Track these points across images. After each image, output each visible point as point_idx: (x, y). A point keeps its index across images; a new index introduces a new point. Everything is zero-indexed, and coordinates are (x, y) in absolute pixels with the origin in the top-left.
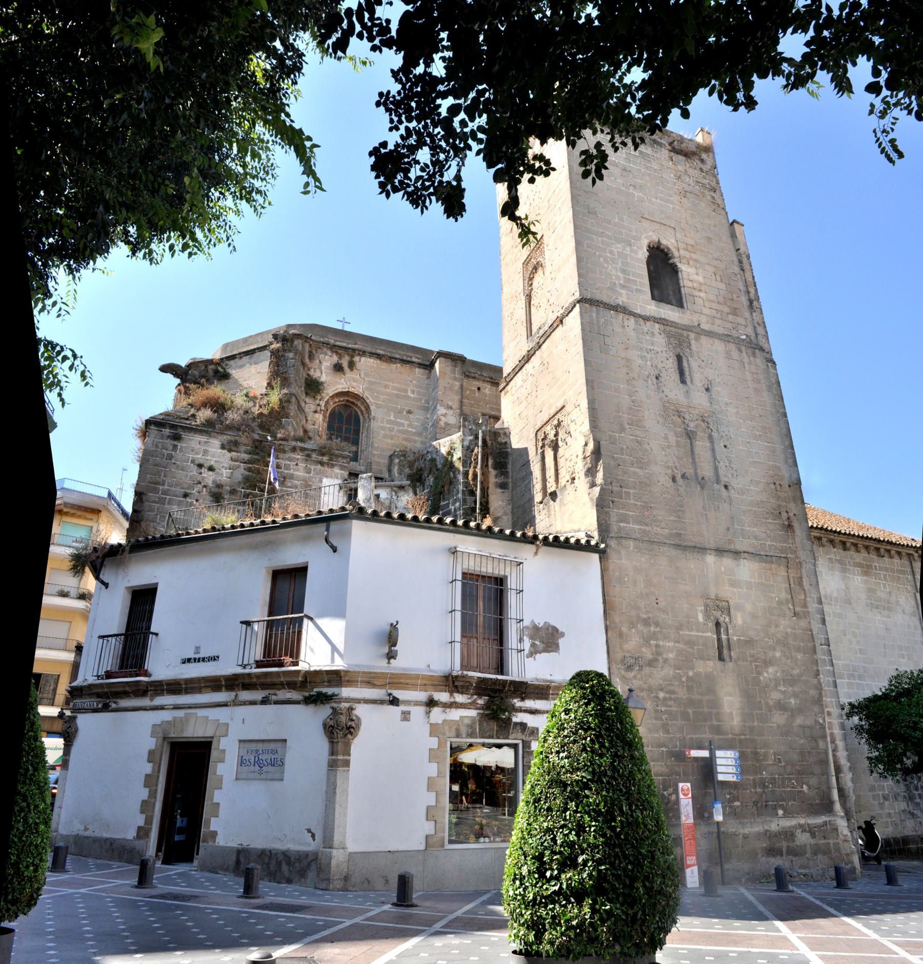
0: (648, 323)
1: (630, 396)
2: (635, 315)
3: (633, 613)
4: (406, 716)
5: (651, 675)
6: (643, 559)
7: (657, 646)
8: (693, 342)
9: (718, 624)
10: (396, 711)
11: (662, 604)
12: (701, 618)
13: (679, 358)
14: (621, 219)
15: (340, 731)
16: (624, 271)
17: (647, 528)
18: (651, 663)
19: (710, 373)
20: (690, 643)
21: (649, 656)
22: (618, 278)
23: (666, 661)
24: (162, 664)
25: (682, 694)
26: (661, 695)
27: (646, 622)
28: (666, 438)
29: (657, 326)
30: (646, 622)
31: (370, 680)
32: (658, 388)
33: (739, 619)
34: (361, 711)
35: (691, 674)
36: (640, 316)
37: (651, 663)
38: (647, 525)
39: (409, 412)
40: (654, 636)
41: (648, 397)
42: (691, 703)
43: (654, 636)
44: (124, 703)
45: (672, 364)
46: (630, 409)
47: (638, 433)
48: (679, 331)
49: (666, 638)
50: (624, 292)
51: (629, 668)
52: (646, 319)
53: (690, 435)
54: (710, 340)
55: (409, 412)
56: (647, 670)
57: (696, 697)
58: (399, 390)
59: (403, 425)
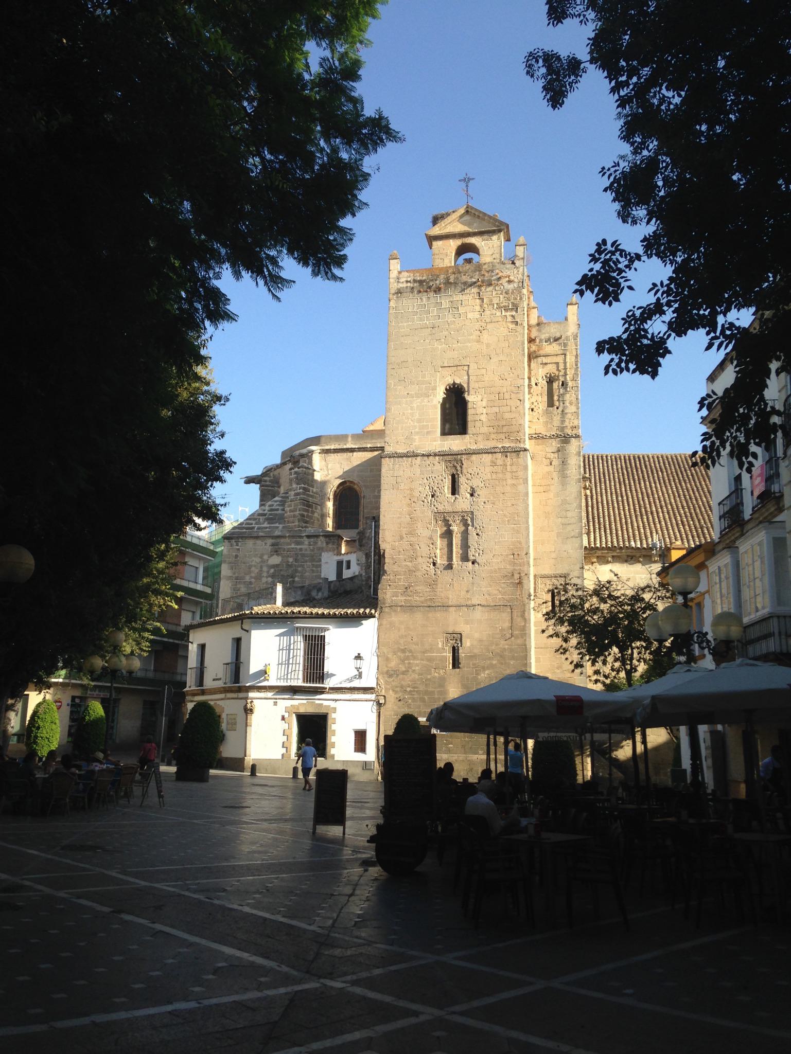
3: (396, 646)
4: (275, 704)
5: (403, 679)
7: (409, 663)
11: (415, 640)
12: (440, 646)
13: (453, 476)
19: (475, 483)
20: (430, 660)
21: (404, 669)
23: (414, 671)
25: (422, 688)
26: (408, 689)
27: (403, 651)
29: (437, 458)
30: (403, 651)
33: (467, 643)
35: (429, 677)
36: (423, 455)
37: (404, 673)
40: (407, 658)
42: (426, 693)
43: (407, 658)
47: (412, 539)
49: (415, 658)
50: (417, 437)
57: (430, 689)
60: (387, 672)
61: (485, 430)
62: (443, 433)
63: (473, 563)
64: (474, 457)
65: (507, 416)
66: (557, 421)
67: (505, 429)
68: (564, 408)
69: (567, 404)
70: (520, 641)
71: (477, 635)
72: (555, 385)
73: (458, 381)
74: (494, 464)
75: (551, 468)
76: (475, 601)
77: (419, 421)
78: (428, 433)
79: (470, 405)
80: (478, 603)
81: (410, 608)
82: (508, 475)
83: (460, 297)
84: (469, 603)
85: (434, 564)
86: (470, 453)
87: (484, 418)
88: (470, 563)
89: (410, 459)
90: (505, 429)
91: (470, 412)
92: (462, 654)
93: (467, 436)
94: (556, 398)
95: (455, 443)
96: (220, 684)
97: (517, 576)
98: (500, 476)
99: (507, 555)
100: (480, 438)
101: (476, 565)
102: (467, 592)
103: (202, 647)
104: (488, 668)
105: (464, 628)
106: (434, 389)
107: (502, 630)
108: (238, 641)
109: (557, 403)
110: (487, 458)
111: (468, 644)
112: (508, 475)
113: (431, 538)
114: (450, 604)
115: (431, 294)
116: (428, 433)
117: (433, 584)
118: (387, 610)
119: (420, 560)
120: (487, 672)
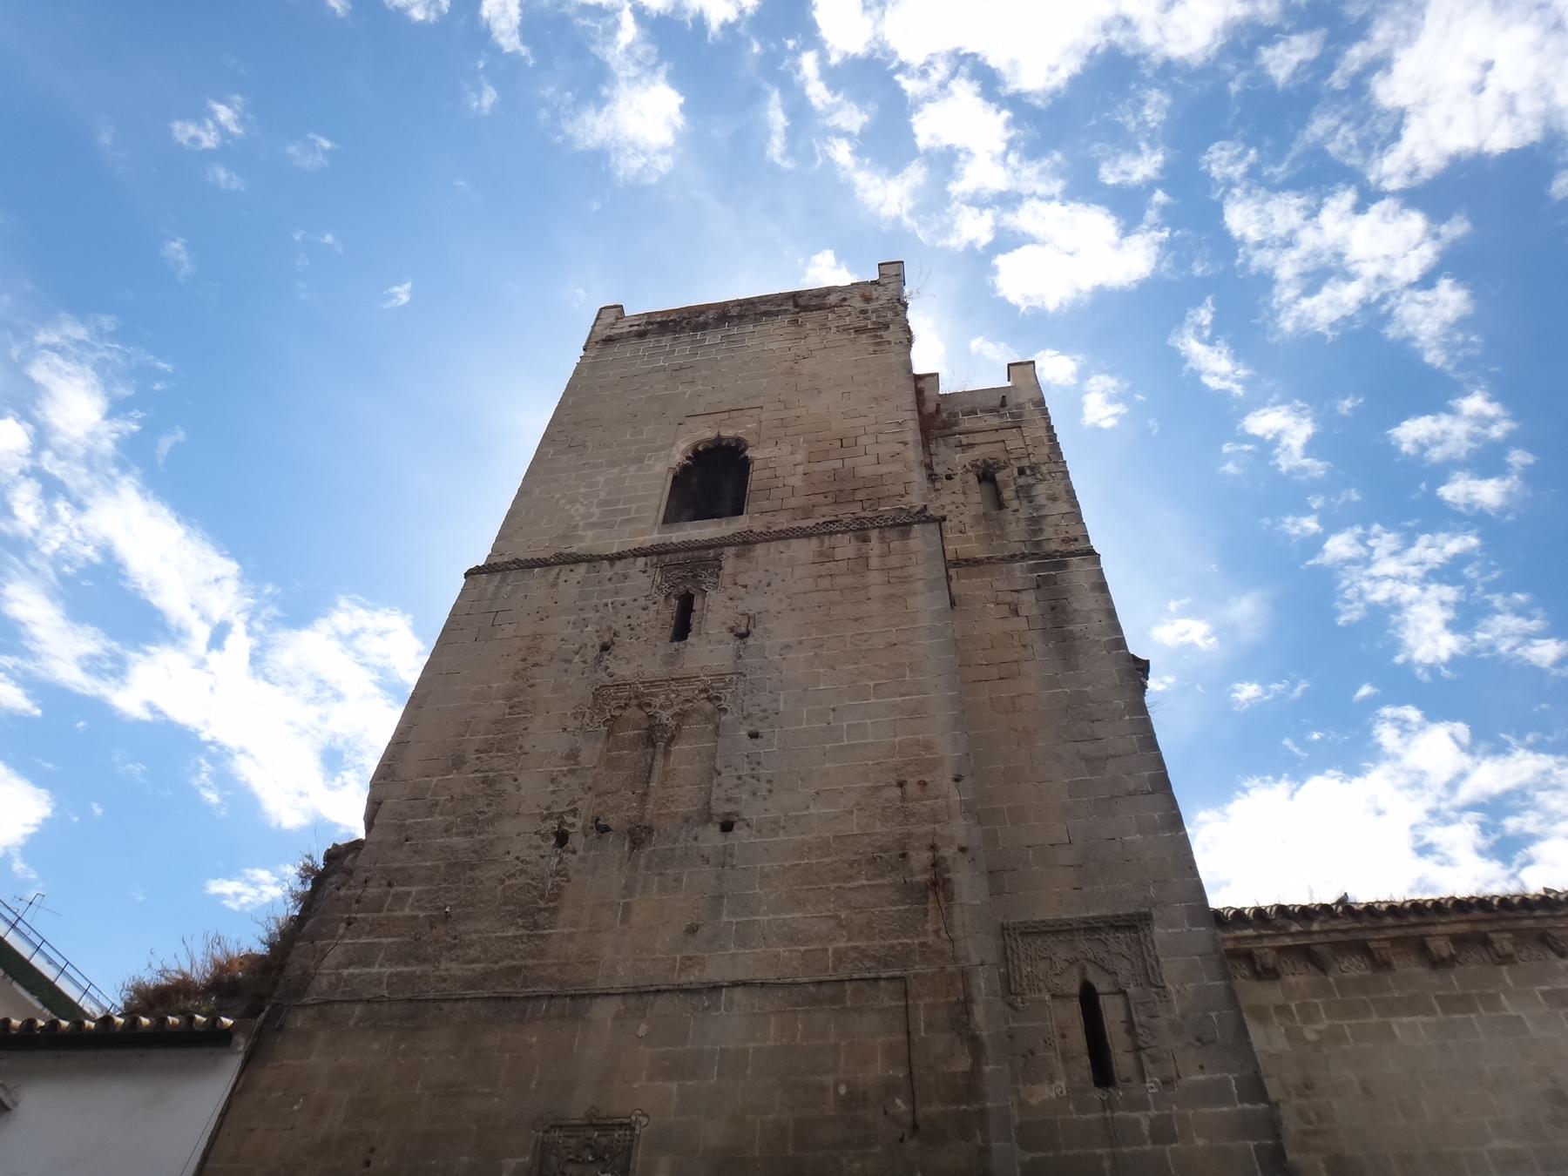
0: (619, 564)
1: (509, 698)
6: (376, 1046)
17: (418, 970)
28: (573, 755)
29: (641, 561)
38: (424, 961)
45: (669, 612)
46: (496, 722)
48: (696, 553)
50: (590, 533)
54: (781, 545)
63: (727, 827)
67: (860, 495)
73: (728, 433)
74: (826, 557)
75: (1021, 624)
76: (713, 972)
80: (731, 976)
82: (875, 578)
84: (693, 977)
85: (562, 838)
86: (745, 542)
88: (713, 830)
89: (556, 569)
90: (860, 495)
98: (847, 580)
99: (877, 789)
102: (692, 930)
110: (803, 549)
112: (875, 578)
113: (573, 755)
114: (601, 984)
117: (536, 906)
118: (299, 1021)
119: (508, 827)
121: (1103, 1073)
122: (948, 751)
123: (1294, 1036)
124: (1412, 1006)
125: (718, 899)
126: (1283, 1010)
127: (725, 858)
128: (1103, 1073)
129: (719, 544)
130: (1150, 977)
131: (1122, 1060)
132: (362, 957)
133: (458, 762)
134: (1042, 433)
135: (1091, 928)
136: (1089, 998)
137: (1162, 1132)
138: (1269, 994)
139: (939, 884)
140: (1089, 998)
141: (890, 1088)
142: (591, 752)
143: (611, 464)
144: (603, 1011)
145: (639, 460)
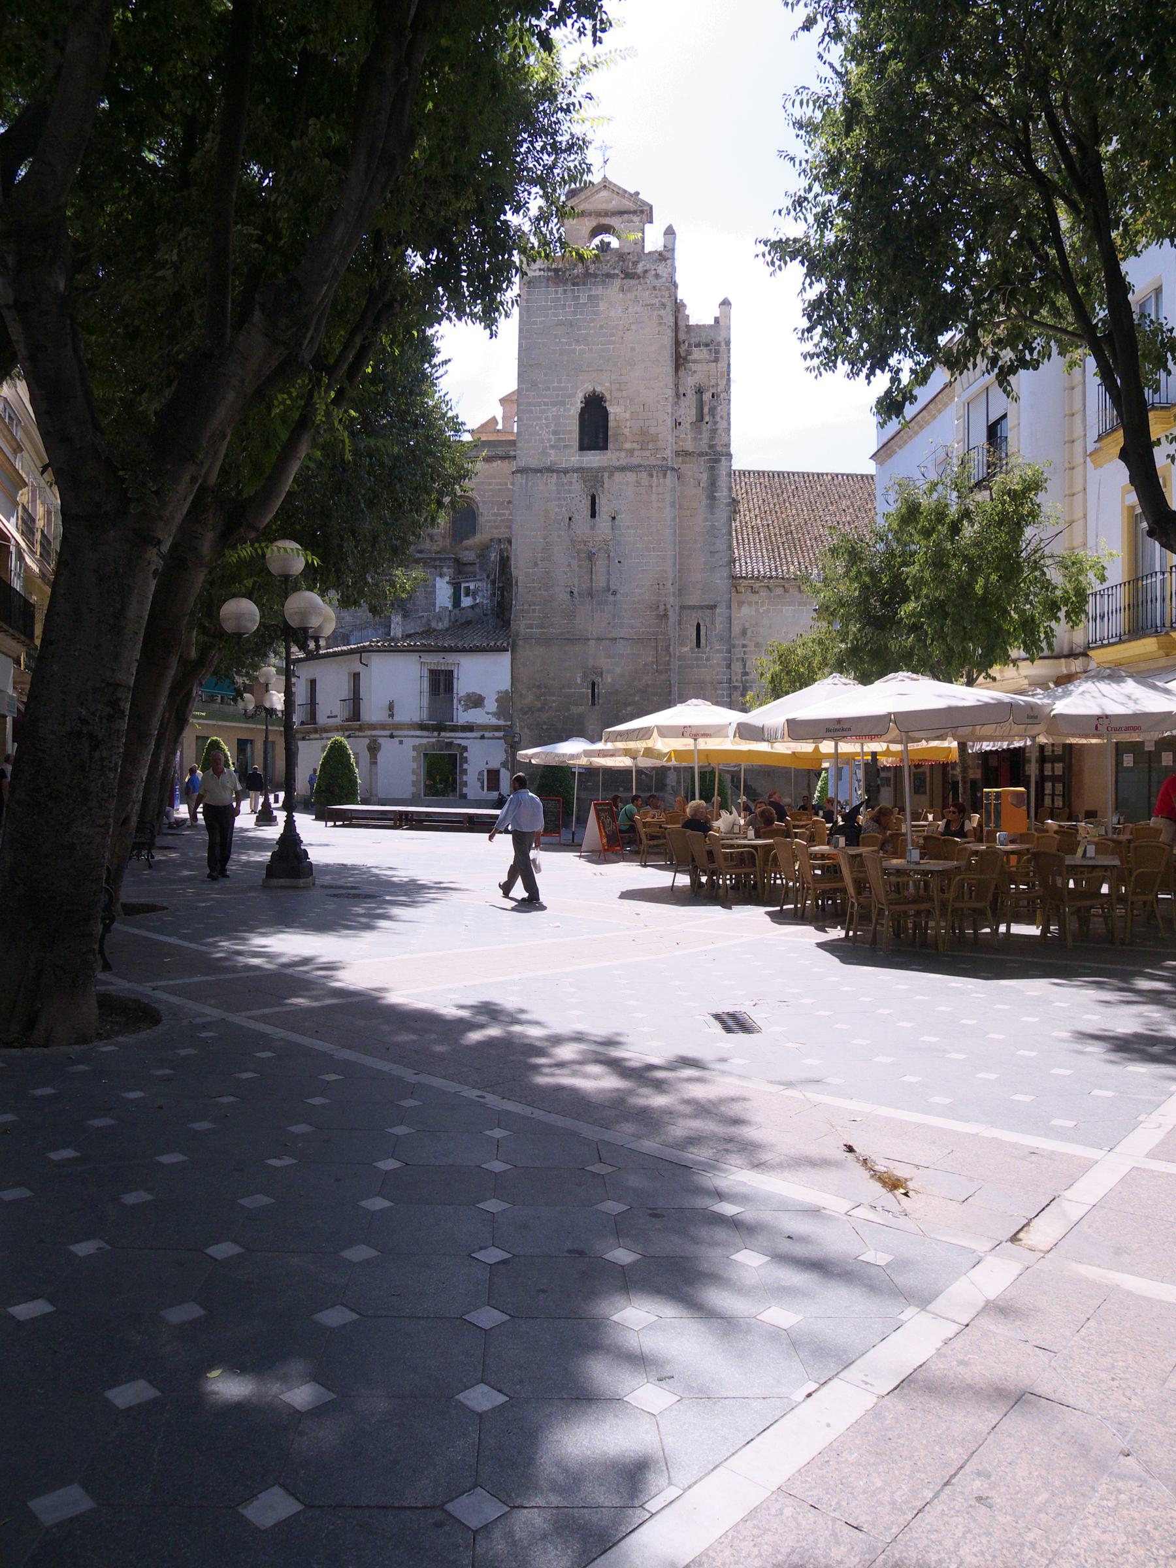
2: (558, 471)
4: (401, 742)
8: (606, 480)
9: (593, 684)
10: (397, 740)
12: (579, 681)
14: (559, 381)
15: (374, 749)
16: (555, 433)
18: (540, 710)
22: (550, 440)
24: (322, 719)
27: (539, 687)
28: (569, 565)
30: (539, 687)
31: (383, 727)
32: (569, 526)
34: (381, 740)
37: (540, 710)
39: (509, 502)
40: (544, 694)
41: (559, 536)
43: (544, 694)
44: (312, 736)
50: (552, 452)
51: (525, 713)
52: (566, 472)
53: (591, 556)
55: (509, 502)
56: (537, 714)
58: (501, 484)
59: (504, 514)
60: (521, 710)
61: (628, 446)
62: (583, 447)
64: (618, 476)
65: (652, 431)
66: (705, 435)
68: (716, 423)
69: (718, 419)
70: (663, 677)
71: (618, 670)
72: (707, 396)
73: (598, 389)
74: (638, 484)
77: (555, 433)
78: (566, 447)
79: (611, 417)
81: (547, 641)
83: (598, 290)
84: (610, 636)
87: (626, 431)
91: (612, 424)
92: (601, 690)
93: (609, 452)
94: (706, 410)
95: (594, 459)
96: (337, 721)
97: (662, 608)
100: (623, 454)
101: (618, 596)
103: (313, 683)
104: (629, 705)
105: (603, 662)
106: (574, 395)
107: (645, 665)
108: (356, 676)
109: (707, 418)
110: (631, 477)
111: (609, 680)
115: (569, 287)
116: (566, 447)
118: (520, 643)
120: (629, 709)
121: (698, 645)
122: (670, 575)
123: (757, 611)
124: (791, 604)
125: (614, 616)
126: (757, 603)
127: (615, 603)
128: (698, 645)
129: (603, 469)
130: (713, 622)
131: (703, 641)
132: (531, 626)
133: (536, 564)
134: (725, 369)
135: (702, 607)
136: (698, 626)
137: (708, 659)
138: (755, 598)
139: (665, 616)
140: (698, 626)
141: (652, 663)
142: (575, 563)
143: (554, 404)
144: (592, 643)
145: (563, 404)
